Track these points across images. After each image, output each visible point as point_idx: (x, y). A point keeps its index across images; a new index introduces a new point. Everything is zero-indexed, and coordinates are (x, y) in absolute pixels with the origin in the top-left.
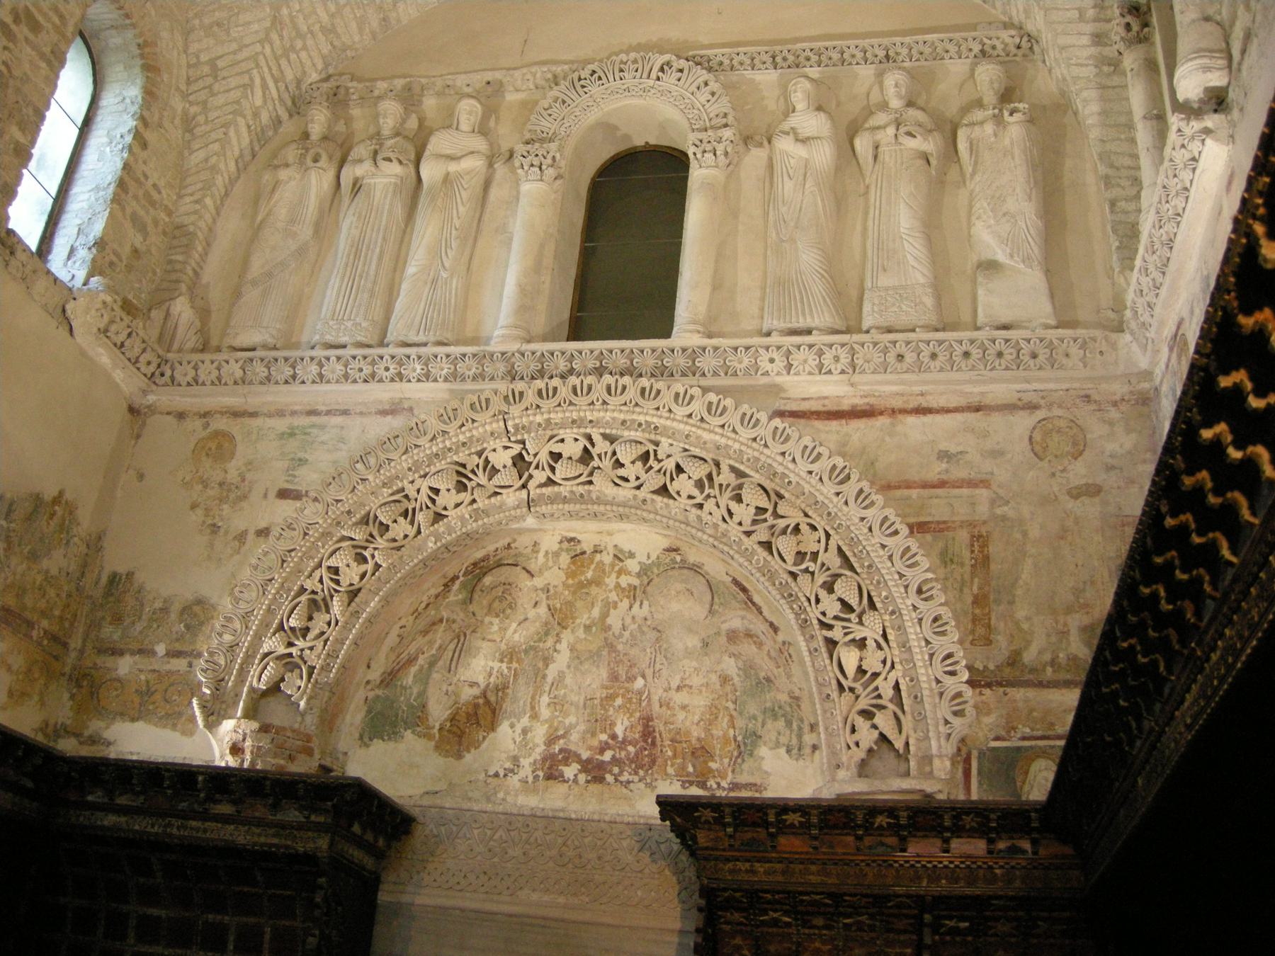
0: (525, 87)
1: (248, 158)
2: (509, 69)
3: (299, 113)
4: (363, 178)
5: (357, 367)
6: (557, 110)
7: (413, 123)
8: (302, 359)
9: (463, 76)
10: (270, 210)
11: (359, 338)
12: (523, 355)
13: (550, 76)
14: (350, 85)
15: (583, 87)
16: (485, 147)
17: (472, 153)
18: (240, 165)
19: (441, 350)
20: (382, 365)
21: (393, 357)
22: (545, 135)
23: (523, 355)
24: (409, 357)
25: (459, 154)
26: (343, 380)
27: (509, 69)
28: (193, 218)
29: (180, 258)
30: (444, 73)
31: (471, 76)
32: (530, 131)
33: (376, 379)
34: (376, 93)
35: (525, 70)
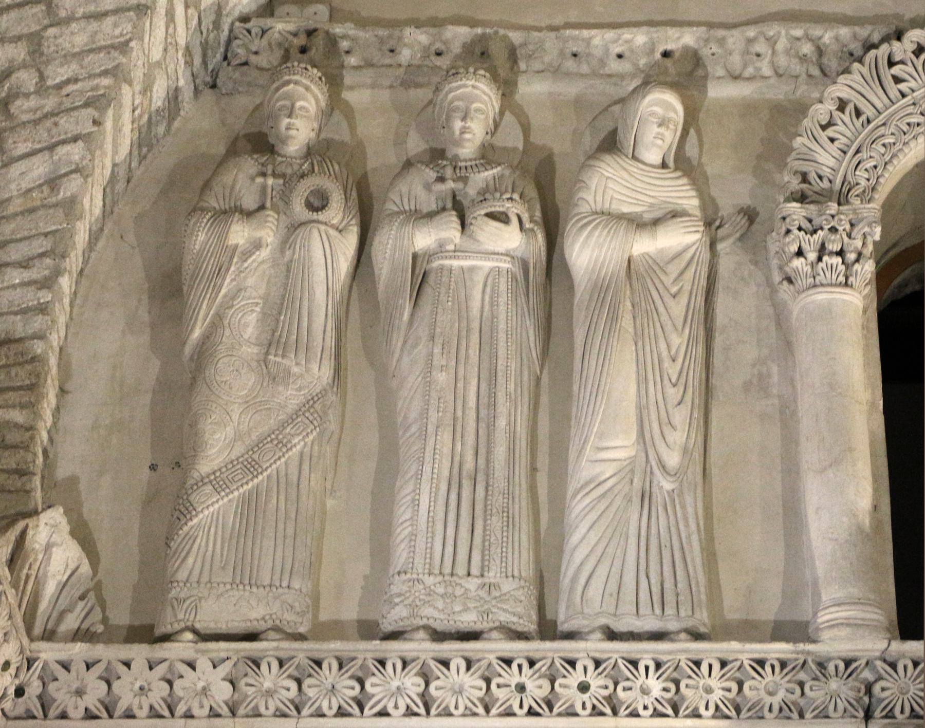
0: (750, 71)
1: (120, 186)
2: (710, 25)
3: (214, 86)
4: (430, 255)
5: (515, 679)
6: (844, 127)
7: (512, 137)
8: (382, 663)
9: (610, 34)
10: (219, 317)
11: (503, 617)
12: (893, 666)
13: (807, 49)
14: (338, 30)
15: (897, 80)
16: (696, 202)
17: (675, 214)
18: (108, 208)
19: (709, 650)
20: (577, 676)
21: (598, 663)
22: (825, 184)
23: (893, 666)
24: (634, 663)
25: (648, 217)
26: (481, 710)
27: (710, 25)
28: (38, 323)
29: (17, 416)
30: (558, 21)
31: (627, 35)
32: (795, 173)
33: (555, 711)
34: (405, 55)
35: (751, 32)
